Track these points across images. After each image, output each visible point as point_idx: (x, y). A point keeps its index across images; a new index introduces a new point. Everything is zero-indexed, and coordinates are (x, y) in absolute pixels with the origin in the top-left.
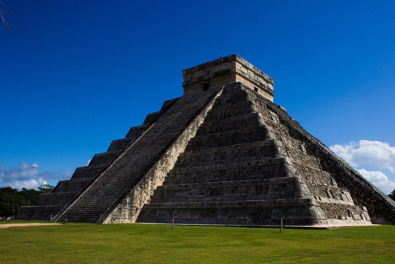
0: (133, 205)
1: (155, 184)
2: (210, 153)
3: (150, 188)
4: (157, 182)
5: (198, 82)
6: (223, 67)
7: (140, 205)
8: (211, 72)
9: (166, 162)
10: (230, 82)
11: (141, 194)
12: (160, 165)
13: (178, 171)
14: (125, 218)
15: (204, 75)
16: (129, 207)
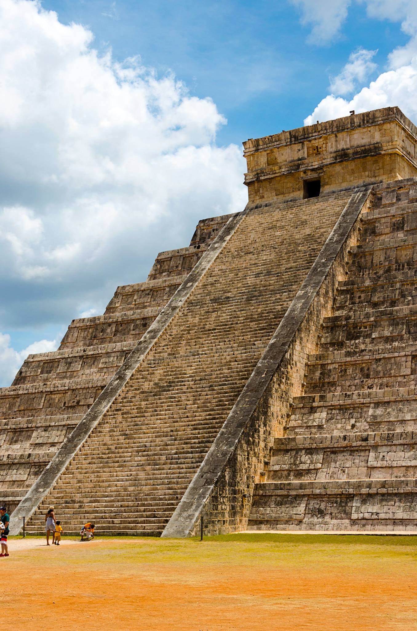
0: (236, 488)
1: (270, 434)
2: (396, 354)
3: (262, 444)
4: (273, 429)
5: (290, 174)
6: (360, 138)
7: (248, 487)
8: (324, 149)
9: (286, 379)
10: (379, 176)
11: (248, 459)
12: (276, 386)
13: (317, 399)
14: (224, 521)
15: (306, 156)
16: (229, 494)
